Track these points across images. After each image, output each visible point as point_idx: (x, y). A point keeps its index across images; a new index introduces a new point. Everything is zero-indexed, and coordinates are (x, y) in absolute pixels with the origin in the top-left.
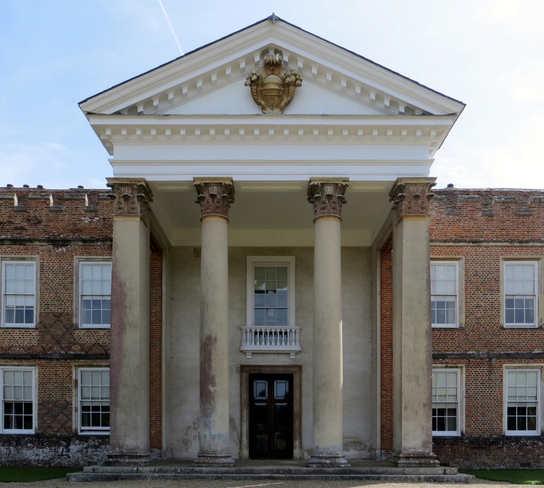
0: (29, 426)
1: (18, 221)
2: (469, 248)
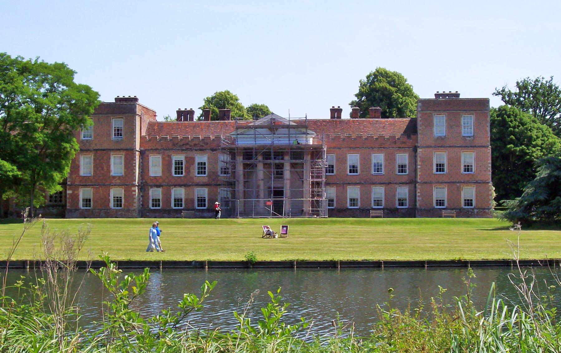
0: (205, 206)
1: (201, 144)
2: (337, 150)
